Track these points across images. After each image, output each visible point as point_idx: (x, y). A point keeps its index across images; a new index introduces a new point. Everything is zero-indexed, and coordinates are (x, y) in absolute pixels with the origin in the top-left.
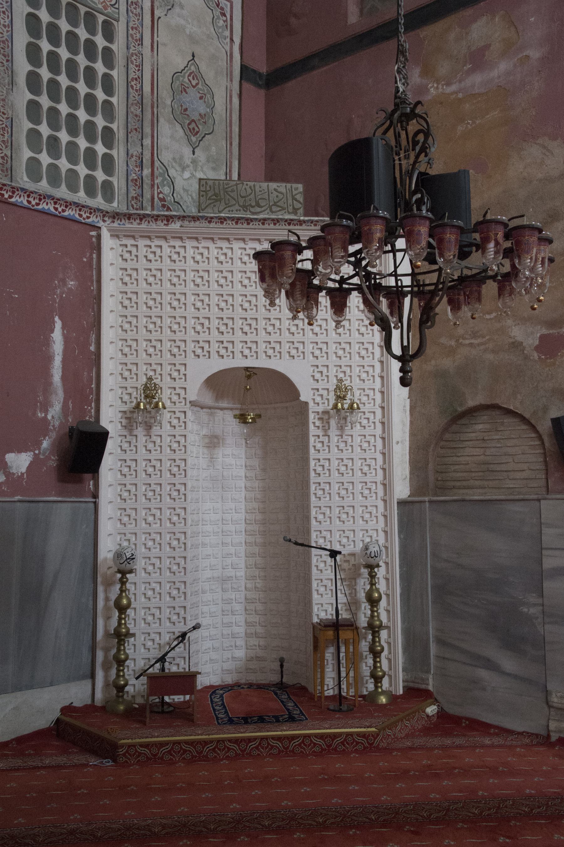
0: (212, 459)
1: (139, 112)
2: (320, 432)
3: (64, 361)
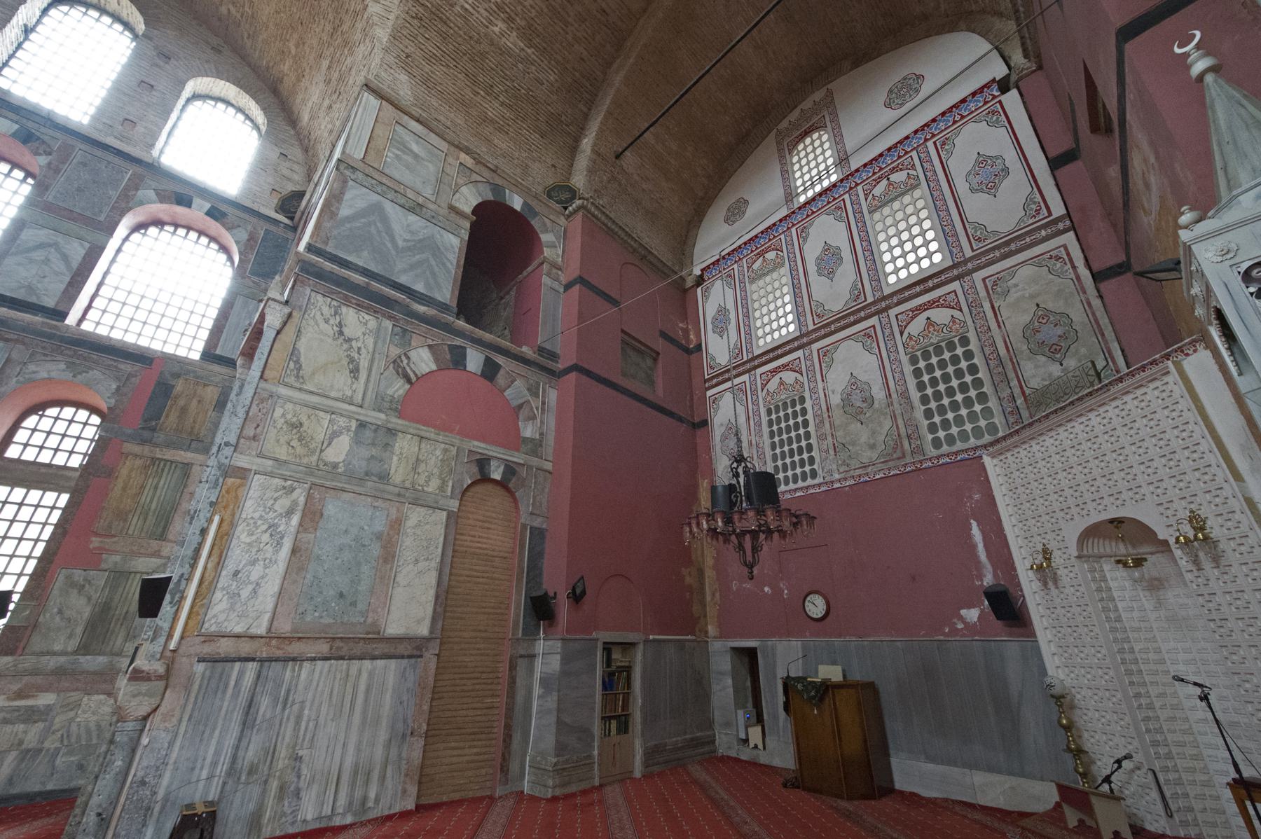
1: (1000, 369)
2: (1191, 567)
3: (985, 546)
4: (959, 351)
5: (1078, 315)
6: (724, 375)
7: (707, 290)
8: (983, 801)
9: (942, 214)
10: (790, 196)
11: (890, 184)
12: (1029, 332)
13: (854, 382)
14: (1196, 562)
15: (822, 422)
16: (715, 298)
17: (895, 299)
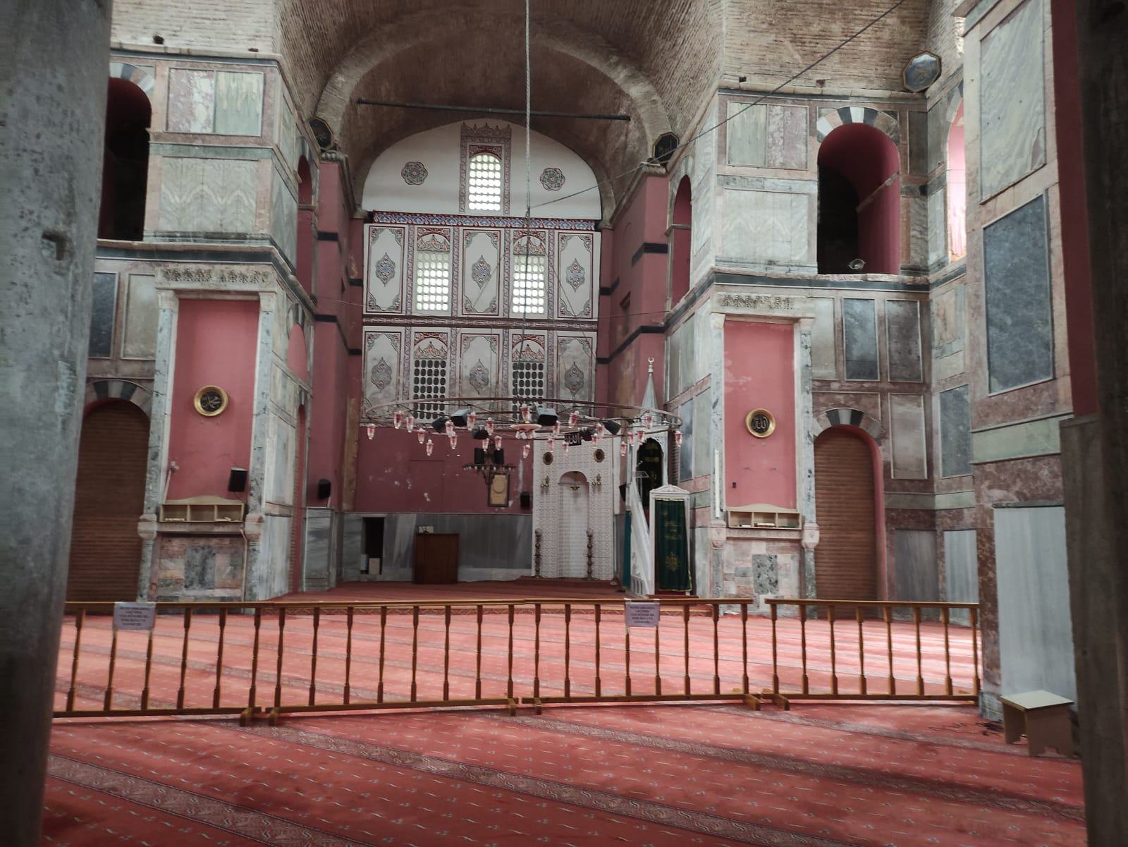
0: (575, 501)
4: (538, 371)
5: (586, 377)
6: (386, 319)
7: (374, 232)
8: (494, 579)
10: (463, 197)
12: (568, 375)
13: (480, 365)
15: (454, 384)
16: (382, 246)
17: (514, 324)
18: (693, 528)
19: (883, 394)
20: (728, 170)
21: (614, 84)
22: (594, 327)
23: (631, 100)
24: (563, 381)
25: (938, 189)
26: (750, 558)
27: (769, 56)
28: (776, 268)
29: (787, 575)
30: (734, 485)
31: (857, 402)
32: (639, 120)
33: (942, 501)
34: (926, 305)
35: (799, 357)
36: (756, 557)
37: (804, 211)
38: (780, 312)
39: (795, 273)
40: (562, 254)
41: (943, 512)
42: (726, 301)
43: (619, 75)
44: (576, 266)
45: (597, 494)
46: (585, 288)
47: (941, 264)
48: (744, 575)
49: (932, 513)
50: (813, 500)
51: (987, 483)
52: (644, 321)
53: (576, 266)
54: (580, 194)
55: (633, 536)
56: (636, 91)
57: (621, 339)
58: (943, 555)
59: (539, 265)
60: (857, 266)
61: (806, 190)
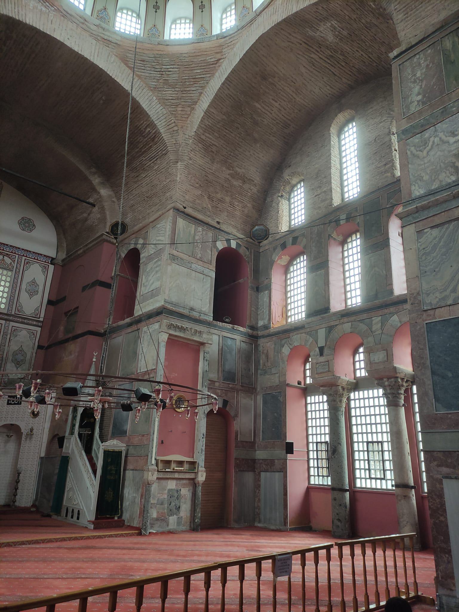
9: (14, 291)
11: (3, 260)
12: (15, 354)
14: (26, 439)
18: (125, 470)
19: (238, 391)
20: (175, 252)
21: (92, 183)
22: (40, 324)
23: (101, 196)
24: (10, 358)
25: (266, 290)
26: (166, 491)
27: (197, 201)
28: (194, 313)
29: (185, 503)
30: (162, 443)
31: (226, 395)
32: (102, 208)
33: (260, 454)
34: (257, 346)
35: (202, 366)
36: (170, 490)
37: (209, 285)
38: (196, 338)
39: (203, 317)
40: (26, 273)
41: (261, 461)
42: (170, 326)
43: (96, 180)
44: (33, 282)
45: (28, 442)
46: (37, 298)
47: (266, 327)
48: (162, 504)
49: (254, 461)
50: (204, 453)
51: (435, 463)
52: (92, 328)
53: (33, 282)
54: (43, 239)
55: (70, 475)
56: (104, 192)
57: (61, 336)
58: (259, 486)
59: (6, 276)
60: (227, 320)
61: (210, 275)
